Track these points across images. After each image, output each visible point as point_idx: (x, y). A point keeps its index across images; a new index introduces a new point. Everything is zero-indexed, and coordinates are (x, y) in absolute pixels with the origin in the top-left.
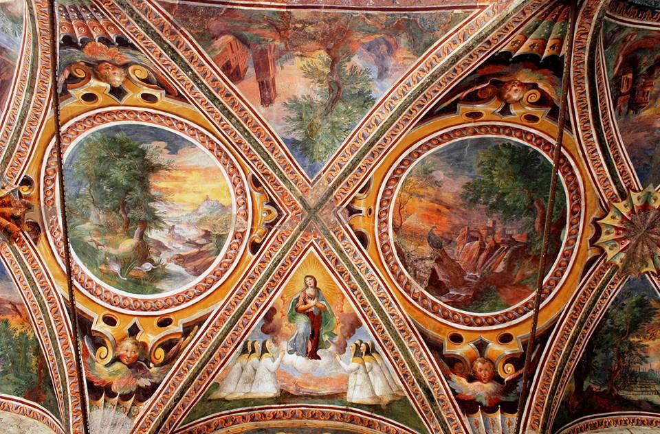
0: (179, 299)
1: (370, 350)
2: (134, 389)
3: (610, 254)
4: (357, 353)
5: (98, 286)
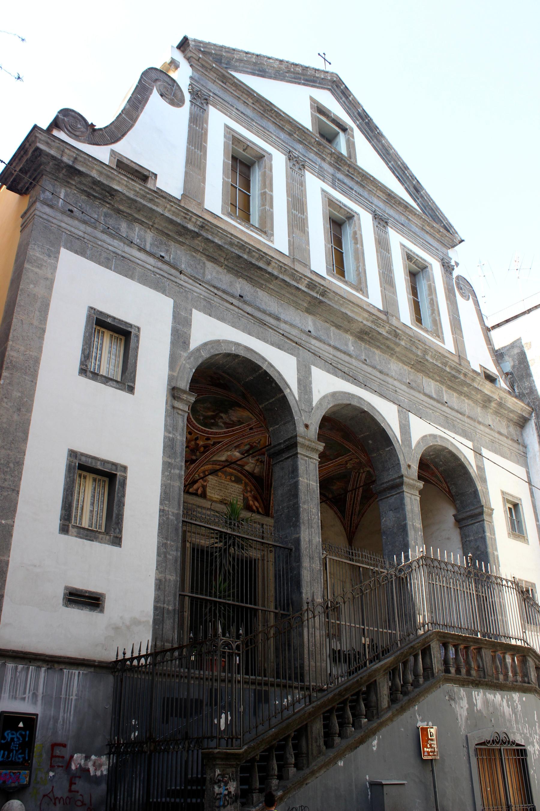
0: (216, 433)
1: (262, 462)
2: (190, 459)
3: (348, 465)
4: (257, 460)
5: (192, 421)
